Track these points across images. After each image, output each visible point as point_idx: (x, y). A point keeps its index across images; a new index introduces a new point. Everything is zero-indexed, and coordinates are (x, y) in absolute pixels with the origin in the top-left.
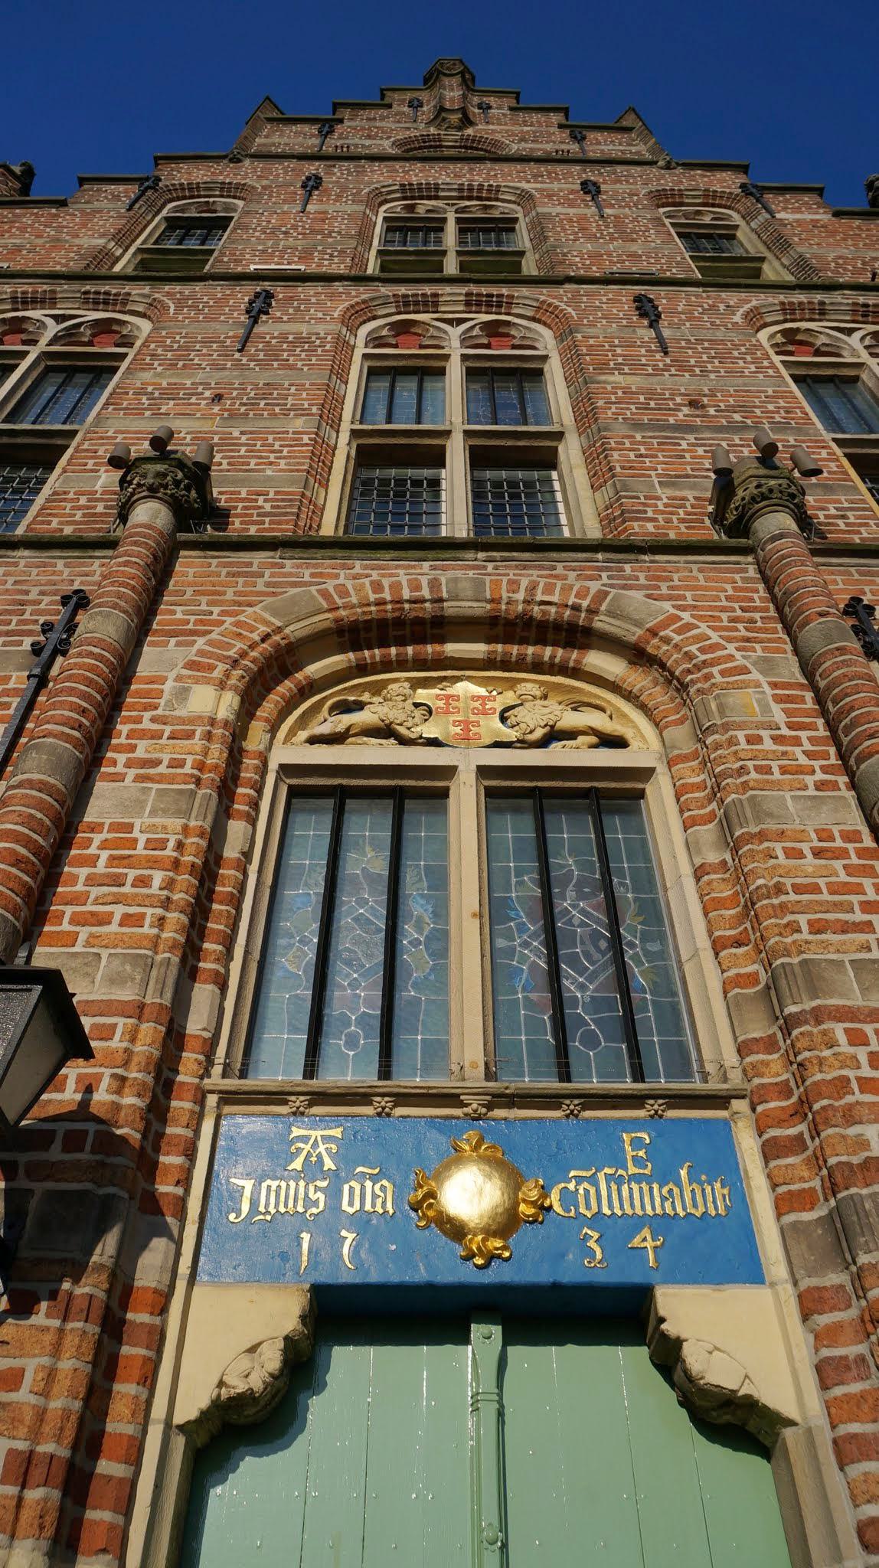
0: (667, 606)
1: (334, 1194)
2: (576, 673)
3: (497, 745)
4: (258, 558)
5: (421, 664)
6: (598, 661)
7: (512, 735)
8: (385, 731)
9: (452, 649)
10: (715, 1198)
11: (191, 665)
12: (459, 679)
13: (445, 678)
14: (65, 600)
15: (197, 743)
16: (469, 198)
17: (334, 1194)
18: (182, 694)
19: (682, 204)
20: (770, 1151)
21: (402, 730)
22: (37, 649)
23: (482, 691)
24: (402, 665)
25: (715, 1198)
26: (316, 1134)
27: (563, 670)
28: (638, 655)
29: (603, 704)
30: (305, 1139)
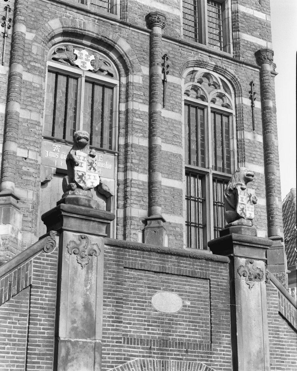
1: (59, 156)
2: (107, 55)
3: (90, 71)
7: (92, 68)
8: (67, 60)
9: (84, 42)
12: (84, 49)
13: (80, 47)
17: (59, 156)
21: (71, 61)
23: (87, 53)
26: (57, 146)
27: (105, 53)
28: (121, 57)
29: (111, 64)
30: (55, 146)
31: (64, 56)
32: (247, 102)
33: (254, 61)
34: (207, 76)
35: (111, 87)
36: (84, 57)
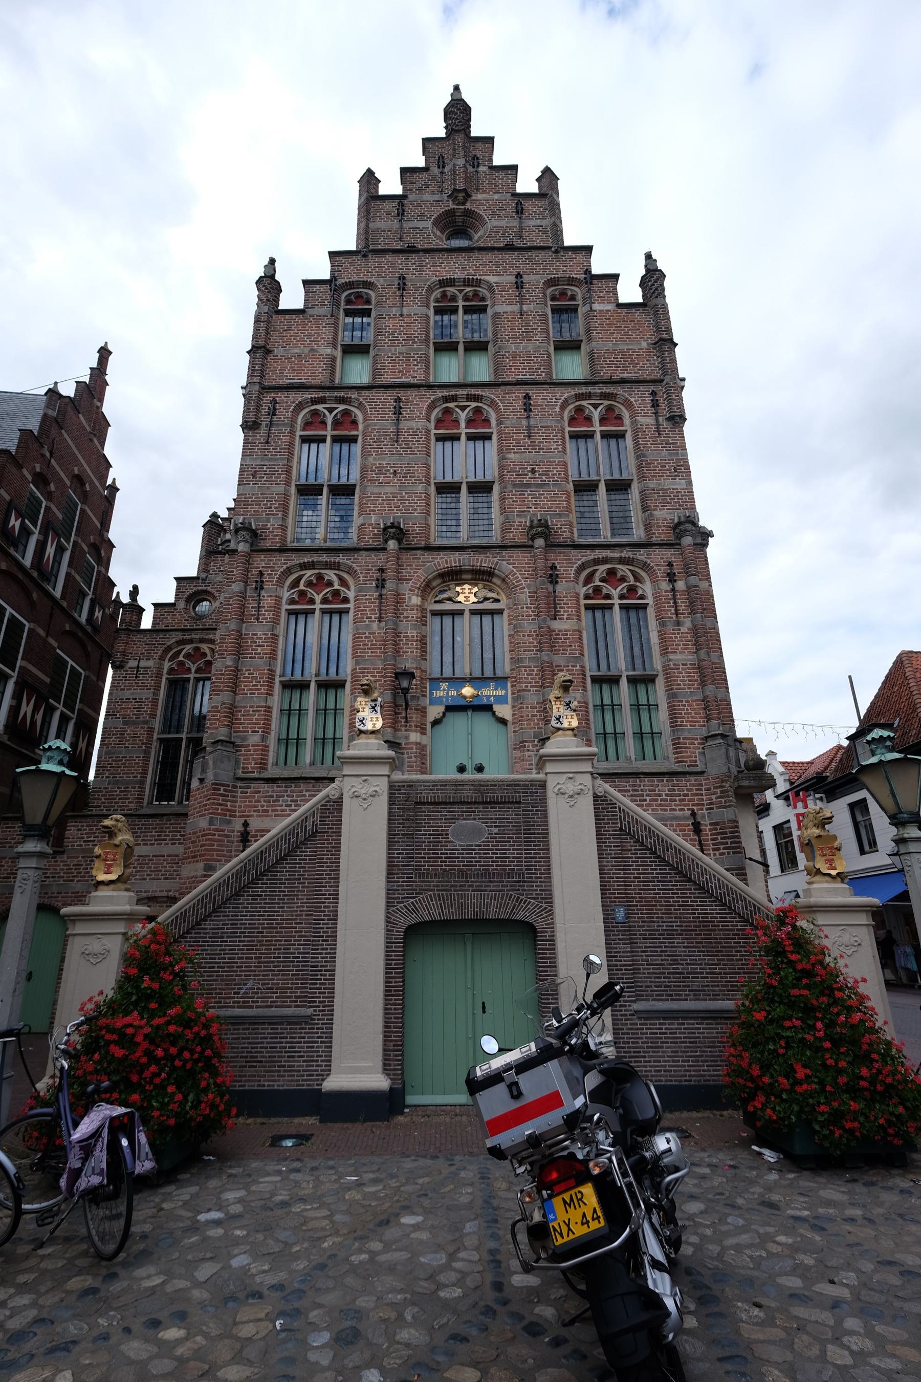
0: (511, 566)
2: (491, 582)
4: (419, 553)
5: (457, 580)
6: (495, 580)
7: (476, 600)
8: (450, 599)
9: (464, 577)
10: (502, 693)
11: (410, 590)
14: (379, 570)
15: (415, 612)
16: (468, 286)
18: (410, 598)
19: (558, 285)
20: (512, 686)
22: (377, 587)
24: (453, 580)
25: (502, 693)
28: (504, 580)
31: (445, 595)
32: (665, 586)
33: (671, 538)
34: (611, 572)
35: (500, 612)
36: (467, 591)
